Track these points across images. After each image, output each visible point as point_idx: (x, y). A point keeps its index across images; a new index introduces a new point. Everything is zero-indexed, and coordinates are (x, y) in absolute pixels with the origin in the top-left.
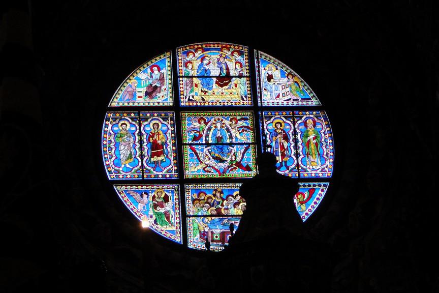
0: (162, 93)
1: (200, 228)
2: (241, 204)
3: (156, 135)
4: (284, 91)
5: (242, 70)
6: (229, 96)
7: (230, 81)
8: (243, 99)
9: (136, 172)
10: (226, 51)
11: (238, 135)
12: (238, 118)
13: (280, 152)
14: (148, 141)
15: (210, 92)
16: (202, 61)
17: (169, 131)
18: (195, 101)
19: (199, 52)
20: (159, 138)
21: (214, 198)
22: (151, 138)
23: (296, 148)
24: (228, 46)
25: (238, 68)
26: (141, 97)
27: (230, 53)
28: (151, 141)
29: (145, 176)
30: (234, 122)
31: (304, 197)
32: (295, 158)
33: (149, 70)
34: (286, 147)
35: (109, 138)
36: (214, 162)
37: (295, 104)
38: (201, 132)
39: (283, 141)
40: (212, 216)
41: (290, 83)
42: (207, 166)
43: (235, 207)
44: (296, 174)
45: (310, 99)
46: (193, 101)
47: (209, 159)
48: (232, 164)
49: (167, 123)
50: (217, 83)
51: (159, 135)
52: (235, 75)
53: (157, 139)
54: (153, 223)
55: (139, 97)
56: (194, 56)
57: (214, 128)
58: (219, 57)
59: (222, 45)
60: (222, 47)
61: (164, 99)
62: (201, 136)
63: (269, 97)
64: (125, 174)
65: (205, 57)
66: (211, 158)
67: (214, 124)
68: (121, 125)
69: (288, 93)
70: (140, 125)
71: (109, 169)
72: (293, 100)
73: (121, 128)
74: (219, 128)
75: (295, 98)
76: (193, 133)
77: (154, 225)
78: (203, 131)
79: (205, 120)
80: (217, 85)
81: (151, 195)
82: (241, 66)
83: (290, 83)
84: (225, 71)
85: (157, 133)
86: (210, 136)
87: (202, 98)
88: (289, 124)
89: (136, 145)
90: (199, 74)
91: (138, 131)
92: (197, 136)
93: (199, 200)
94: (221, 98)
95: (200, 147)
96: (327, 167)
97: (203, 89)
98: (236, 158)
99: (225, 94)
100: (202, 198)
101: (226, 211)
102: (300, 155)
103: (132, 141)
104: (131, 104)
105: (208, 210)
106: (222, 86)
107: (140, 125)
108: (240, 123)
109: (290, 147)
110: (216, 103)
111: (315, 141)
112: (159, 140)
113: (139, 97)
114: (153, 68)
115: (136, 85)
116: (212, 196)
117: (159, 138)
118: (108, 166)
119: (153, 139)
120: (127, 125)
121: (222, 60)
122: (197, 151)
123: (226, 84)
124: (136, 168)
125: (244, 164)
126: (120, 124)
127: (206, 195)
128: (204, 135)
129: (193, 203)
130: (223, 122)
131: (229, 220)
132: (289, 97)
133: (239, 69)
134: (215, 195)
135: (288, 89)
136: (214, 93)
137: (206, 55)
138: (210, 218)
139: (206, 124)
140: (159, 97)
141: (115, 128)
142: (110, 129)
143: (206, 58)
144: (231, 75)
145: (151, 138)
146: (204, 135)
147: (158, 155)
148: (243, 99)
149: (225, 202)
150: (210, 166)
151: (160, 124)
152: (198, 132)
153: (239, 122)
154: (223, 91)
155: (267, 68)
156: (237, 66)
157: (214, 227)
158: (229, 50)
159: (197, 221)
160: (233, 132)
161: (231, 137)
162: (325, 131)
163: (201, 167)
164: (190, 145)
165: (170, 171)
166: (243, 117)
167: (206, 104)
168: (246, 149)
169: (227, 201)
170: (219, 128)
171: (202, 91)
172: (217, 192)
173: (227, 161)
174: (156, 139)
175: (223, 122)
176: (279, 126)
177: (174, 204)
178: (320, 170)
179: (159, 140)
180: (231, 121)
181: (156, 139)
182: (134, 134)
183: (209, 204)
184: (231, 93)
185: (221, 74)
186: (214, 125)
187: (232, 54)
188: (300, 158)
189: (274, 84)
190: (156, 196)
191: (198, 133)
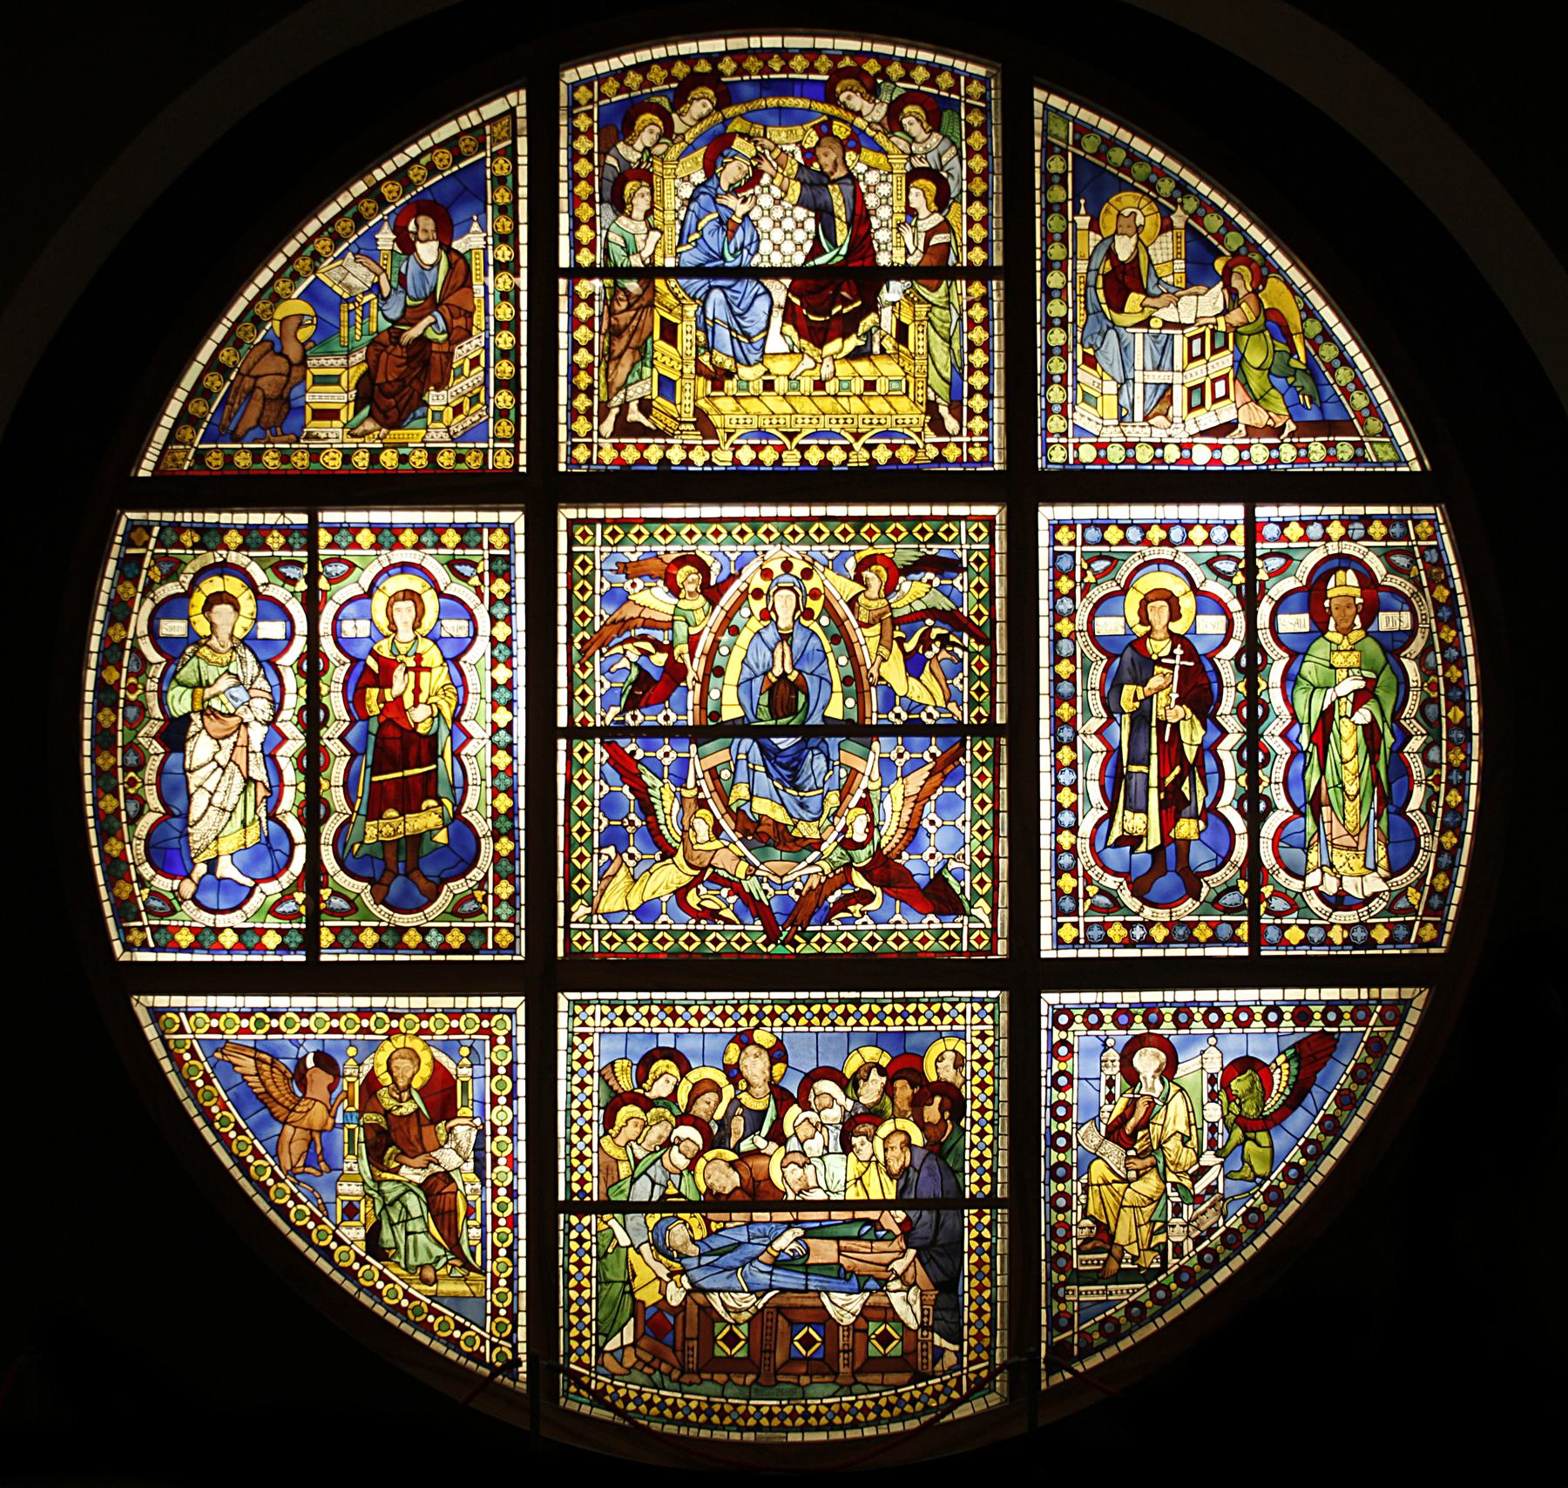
0: (459, 386)
1: (637, 1283)
2: (886, 1128)
3: (398, 673)
4: (1197, 373)
5: (946, 226)
6: (856, 405)
7: (871, 306)
8: (937, 425)
9: (272, 911)
10: (857, 102)
11: (894, 671)
12: (906, 554)
13: (1154, 781)
14: (355, 703)
15: (744, 372)
16: (710, 169)
17: (482, 645)
18: (658, 433)
19: (700, 105)
20: (417, 691)
21: (728, 1092)
22: (373, 693)
23: (1253, 755)
24: (872, 67)
25: (923, 213)
26: (333, 415)
27: (879, 112)
28: (374, 707)
29: (326, 938)
30: (875, 578)
31: (1266, 1094)
32: (1239, 825)
33: (386, 238)
34: (1190, 753)
35: (131, 688)
36: (740, 848)
37: (1259, 454)
38: (682, 649)
39: (1178, 713)
40: (712, 1202)
41: (1235, 317)
42: (695, 882)
43: (847, 1148)
44: (1236, 925)
45: (1346, 427)
46: (646, 432)
47: (717, 830)
48: (848, 867)
49: (470, 598)
50: (790, 314)
51: (418, 669)
52: (899, 260)
53: (408, 700)
54: (360, 1248)
55: (320, 415)
56: (668, 132)
57: (755, 625)
58: (812, 139)
59: (836, 57)
60: (837, 74)
61: (458, 426)
62: (674, 672)
63: (1109, 407)
64: (206, 919)
65: (733, 135)
66: (727, 825)
67: (758, 594)
68: (207, 607)
69: (1220, 392)
70: (312, 604)
71: (123, 890)
72: (1251, 431)
73: (202, 628)
74: (785, 622)
75: (1258, 417)
76: (633, 655)
77: (362, 1261)
78: (693, 641)
79: (704, 569)
80: (789, 329)
81: (354, 1077)
82: (942, 201)
83: (1235, 317)
84: (843, 235)
85: (411, 662)
86: (732, 674)
87: (698, 411)
88: (1223, 609)
89: (285, 738)
90: (691, 258)
91: (299, 645)
92: (655, 675)
93: (646, 1104)
94: (808, 414)
95: (666, 753)
96: (1419, 884)
97: (705, 359)
98: (871, 826)
99: (831, 387)
100: (661, 1089)
101: (794, 1173)
102: (1271, 807)
103: (262, 708)
104: (271, 461)
105: (691, 1168)
106: (818, 337)
107: (312, 604)
108: (915, 592)
109: (1213, 750)
110: (781, 449)
111: (1363, 716)
112: (416, 703)
113: (320, 415)
114: (412, 227)
115: (305, 334)
116: (721, 1078)
117: (417, 691)
118: (117, 868)
119: (381, 699)
120: (237, 608)
121: (827, 159)
122: (648, 778)
123: (847, 326)
124: (273, 889)
125: (918, 866)
126: (198, 600)
127: (685, 1068)
128: (696, 668)
129: (609, 1122)
130: (809, 585)
131: (809, 1233)
132: (1226, 413)
133: (929, 221)
134: (734, 1073)
135: (1224, 362)
136: (769, 386)
137: (737, 126)
138: (696, 1220)
139: (712, 593)
140: (438, 417)
141: (172, 628)
142: (143, 628)
143: (738, 143)
144: (883, 260)
145: (373, 693)
146: (696, 668)
147: (409, 798)
148: (937, 425)
149: (794, 1110)
150: (715, 878)
151: (431, 601)
152: (659, 646)
153: (904, 584)
154: (826, 371)
155: (1108, 222)
156: (917, 201)
157: (720, 1281)
158: (873, 93)
159: (624, 1240)
160: (868, 641)
161: (855, 682)
162: (1428, 648)
163: (667, 878)
164: (608, 734)
165: (469, 906)
166: (935, 549)
167: (723, 458)
168: (947, 770)
169: (806, 1107)
170: (785, 622)
171: (700, 371)
172: (751, 1049)
173: (816, 845)
174: (399, 699)
175: (809, 585)
176: (1159, 612)
177: (481, 1133)
178: (1378, 905)
179: (416, 703)
180: (858, 579)
181: (399, 699)
182: (269, 665)
183: (700, 1124)
184: (870, 385)
185: (817, 250)
186: (758, 605)
187: (893, 122)
188: (1268, 829)
189: (1145, 324)
190: (386, 1079)
191: (660, 659)
